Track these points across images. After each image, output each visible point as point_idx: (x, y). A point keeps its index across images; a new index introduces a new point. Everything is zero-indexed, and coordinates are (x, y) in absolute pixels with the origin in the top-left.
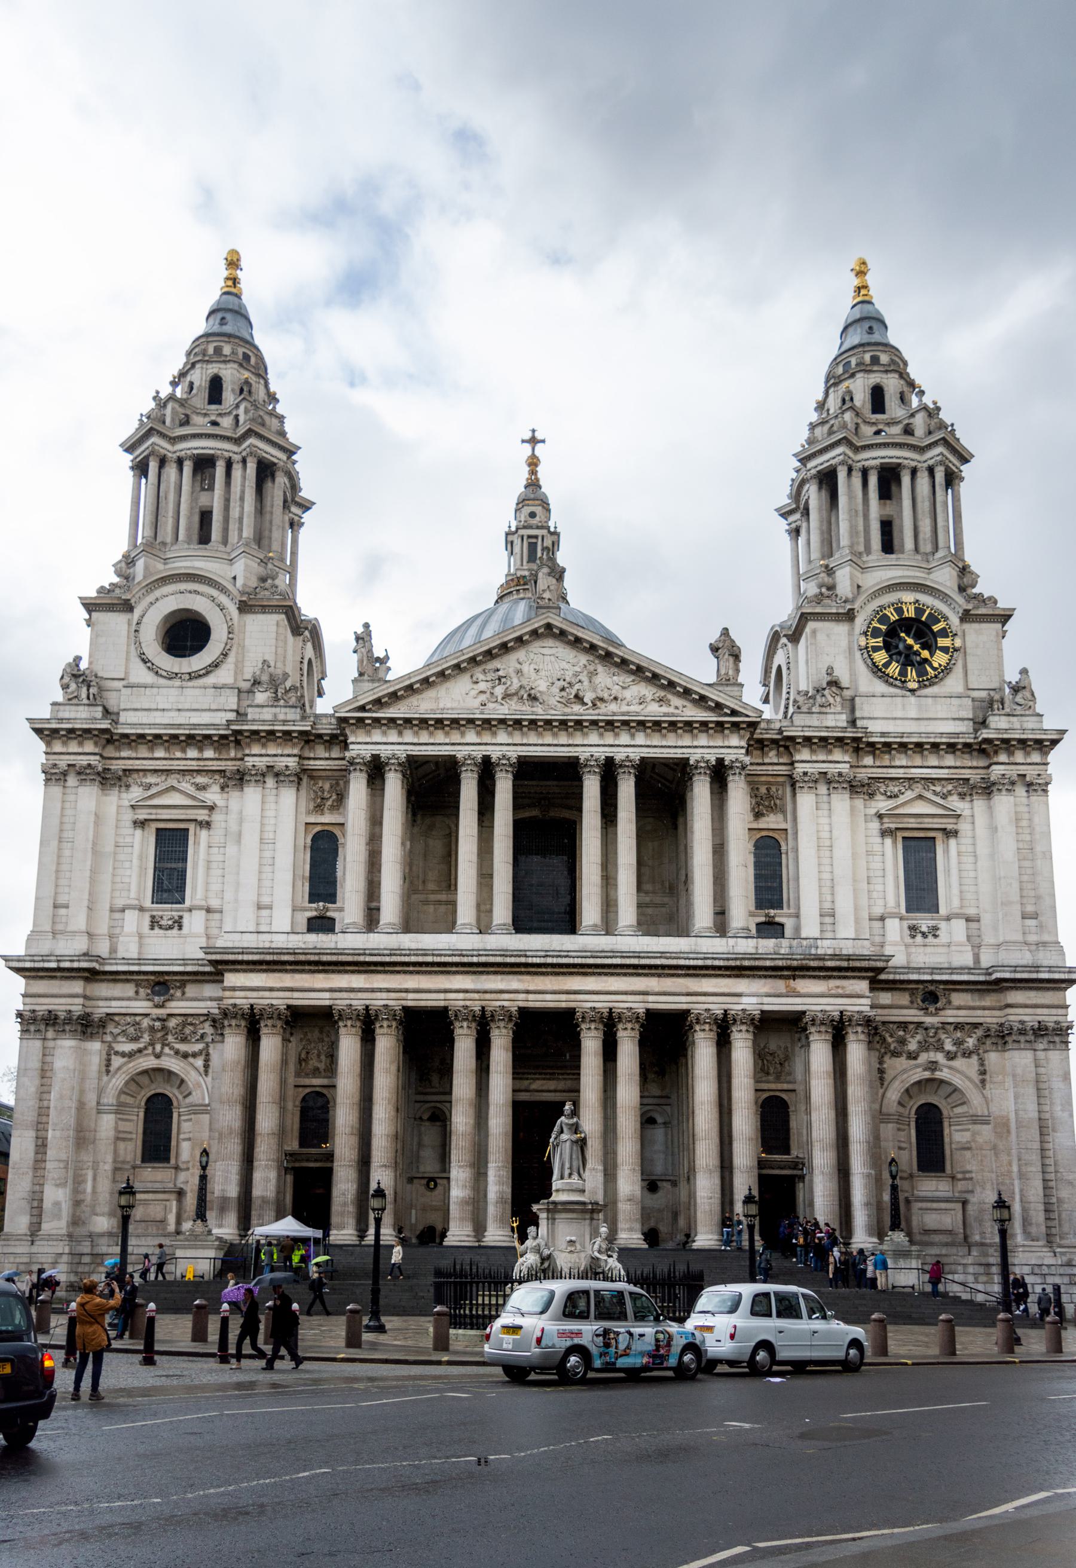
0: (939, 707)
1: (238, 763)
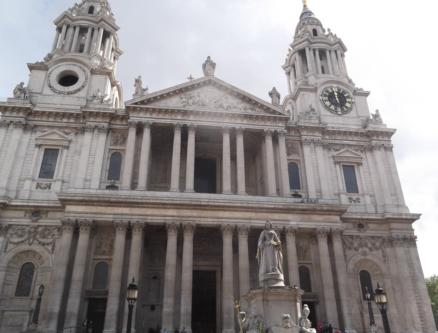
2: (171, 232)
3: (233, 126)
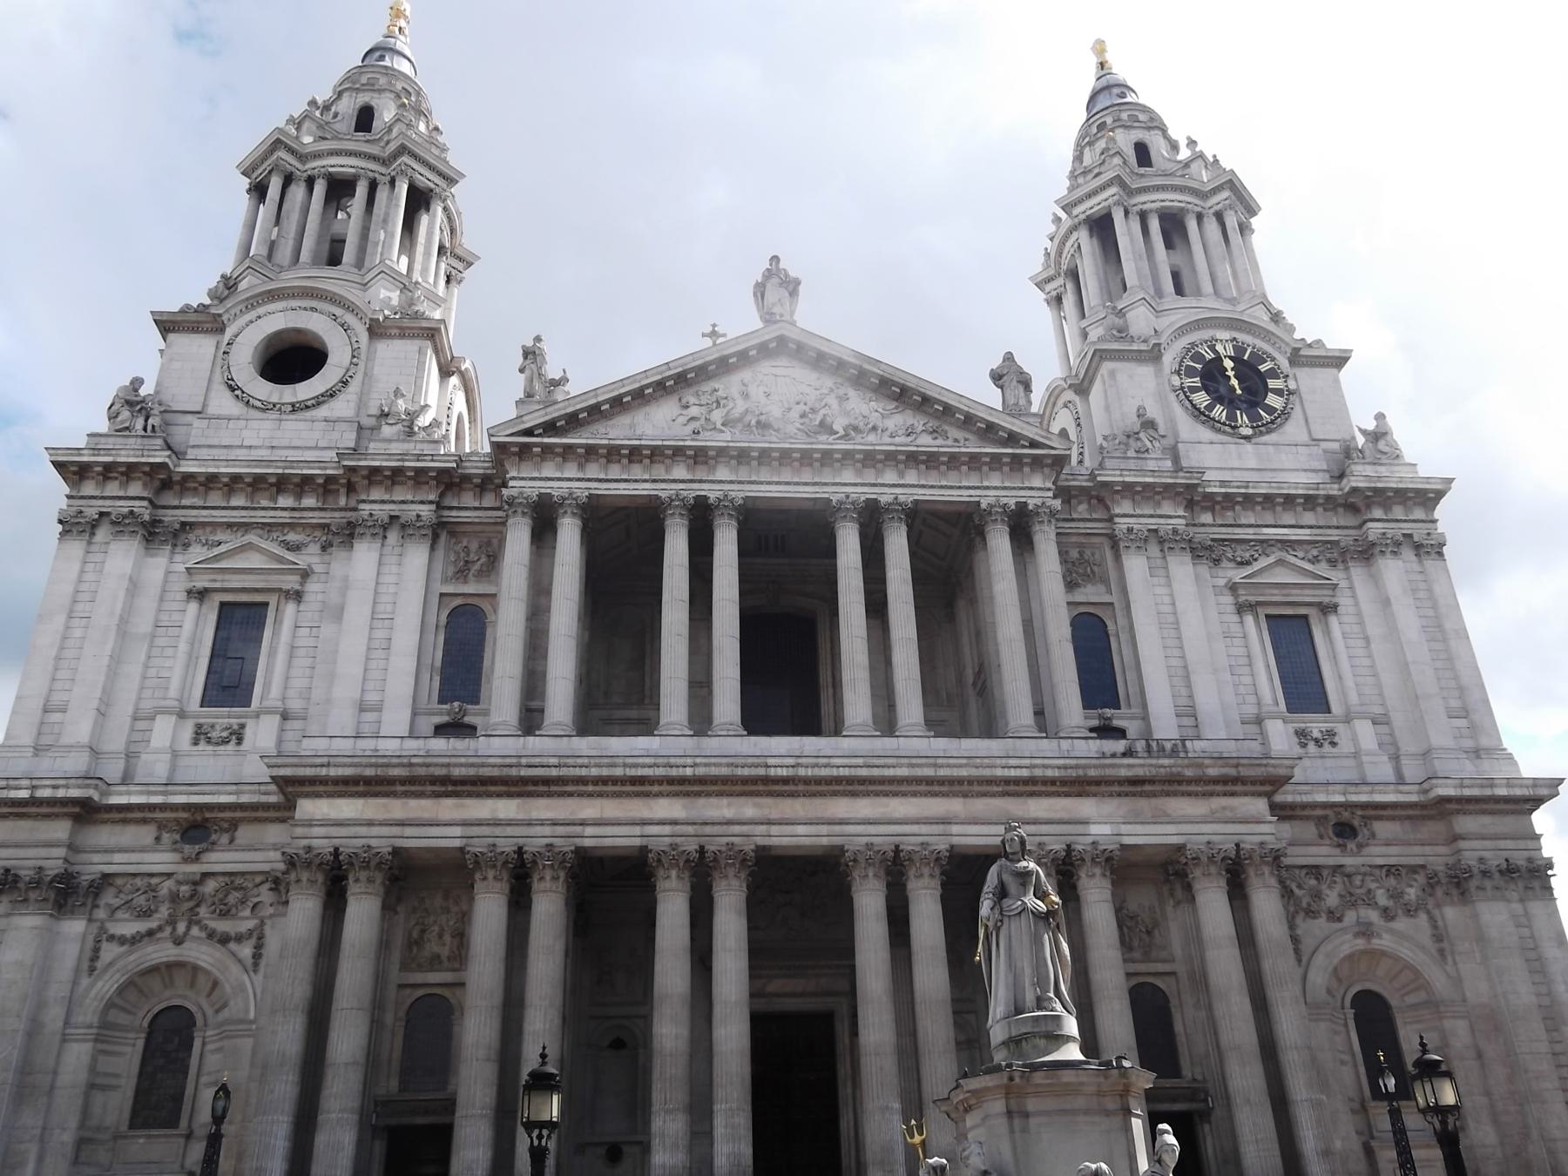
1: (349, 514)
2: (668, 877)
3: (868, 496)
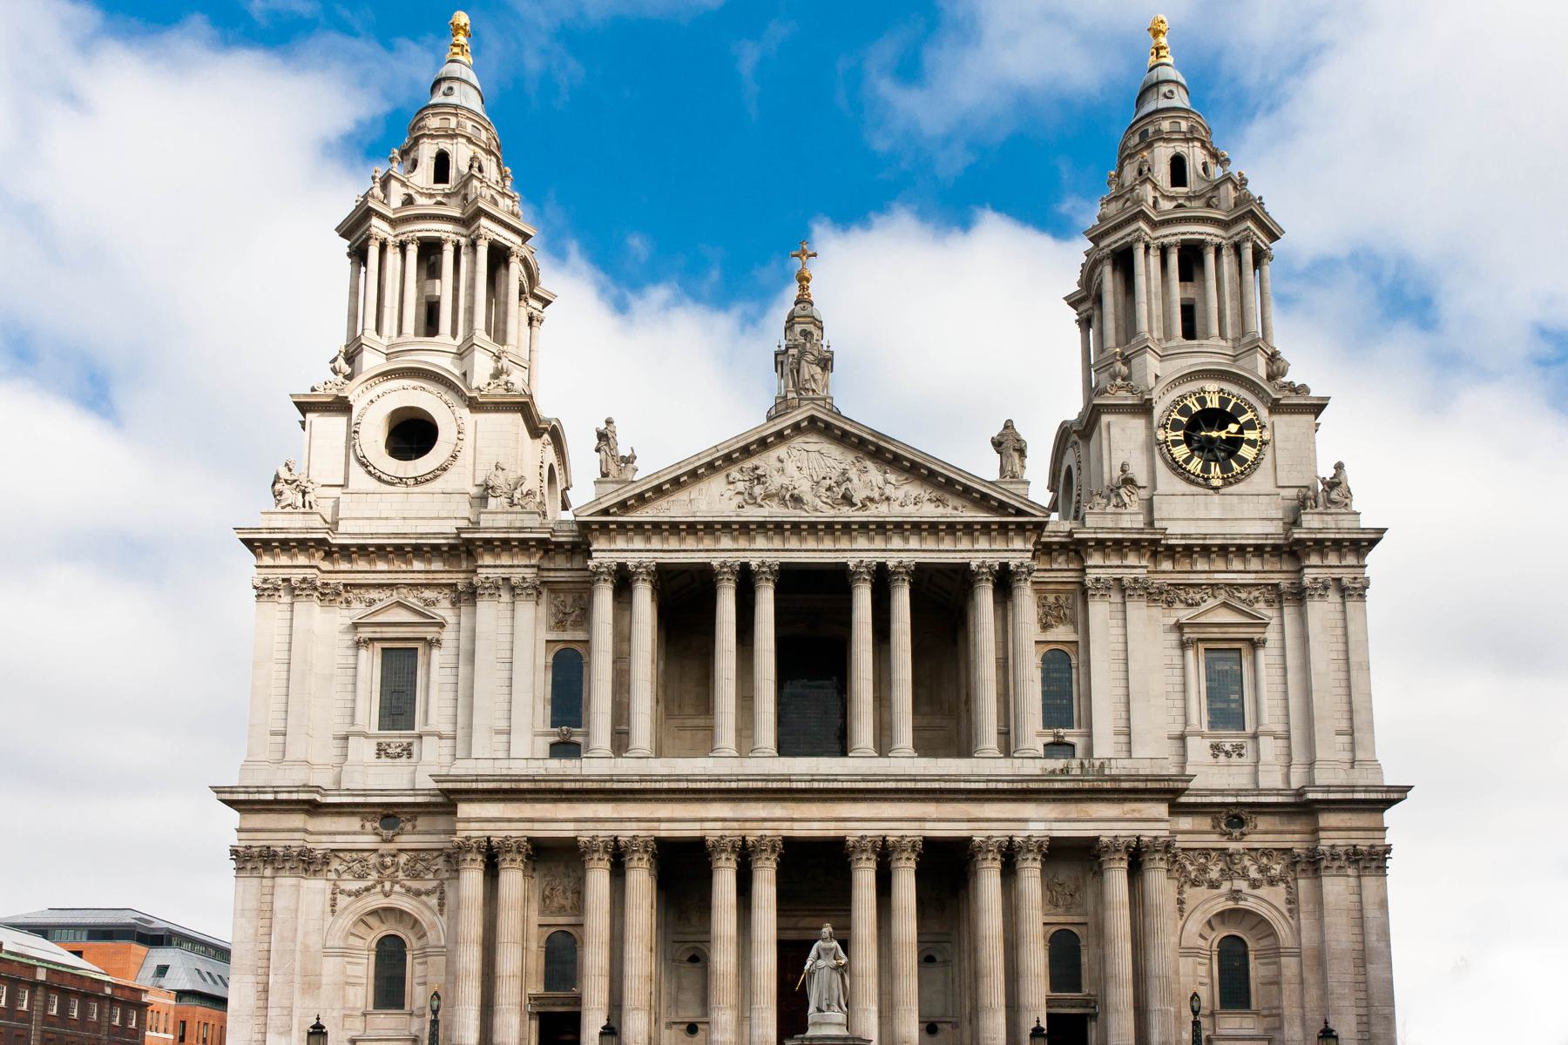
0: (1245, 506)
1: (470, 575)
3: (879, 560)
